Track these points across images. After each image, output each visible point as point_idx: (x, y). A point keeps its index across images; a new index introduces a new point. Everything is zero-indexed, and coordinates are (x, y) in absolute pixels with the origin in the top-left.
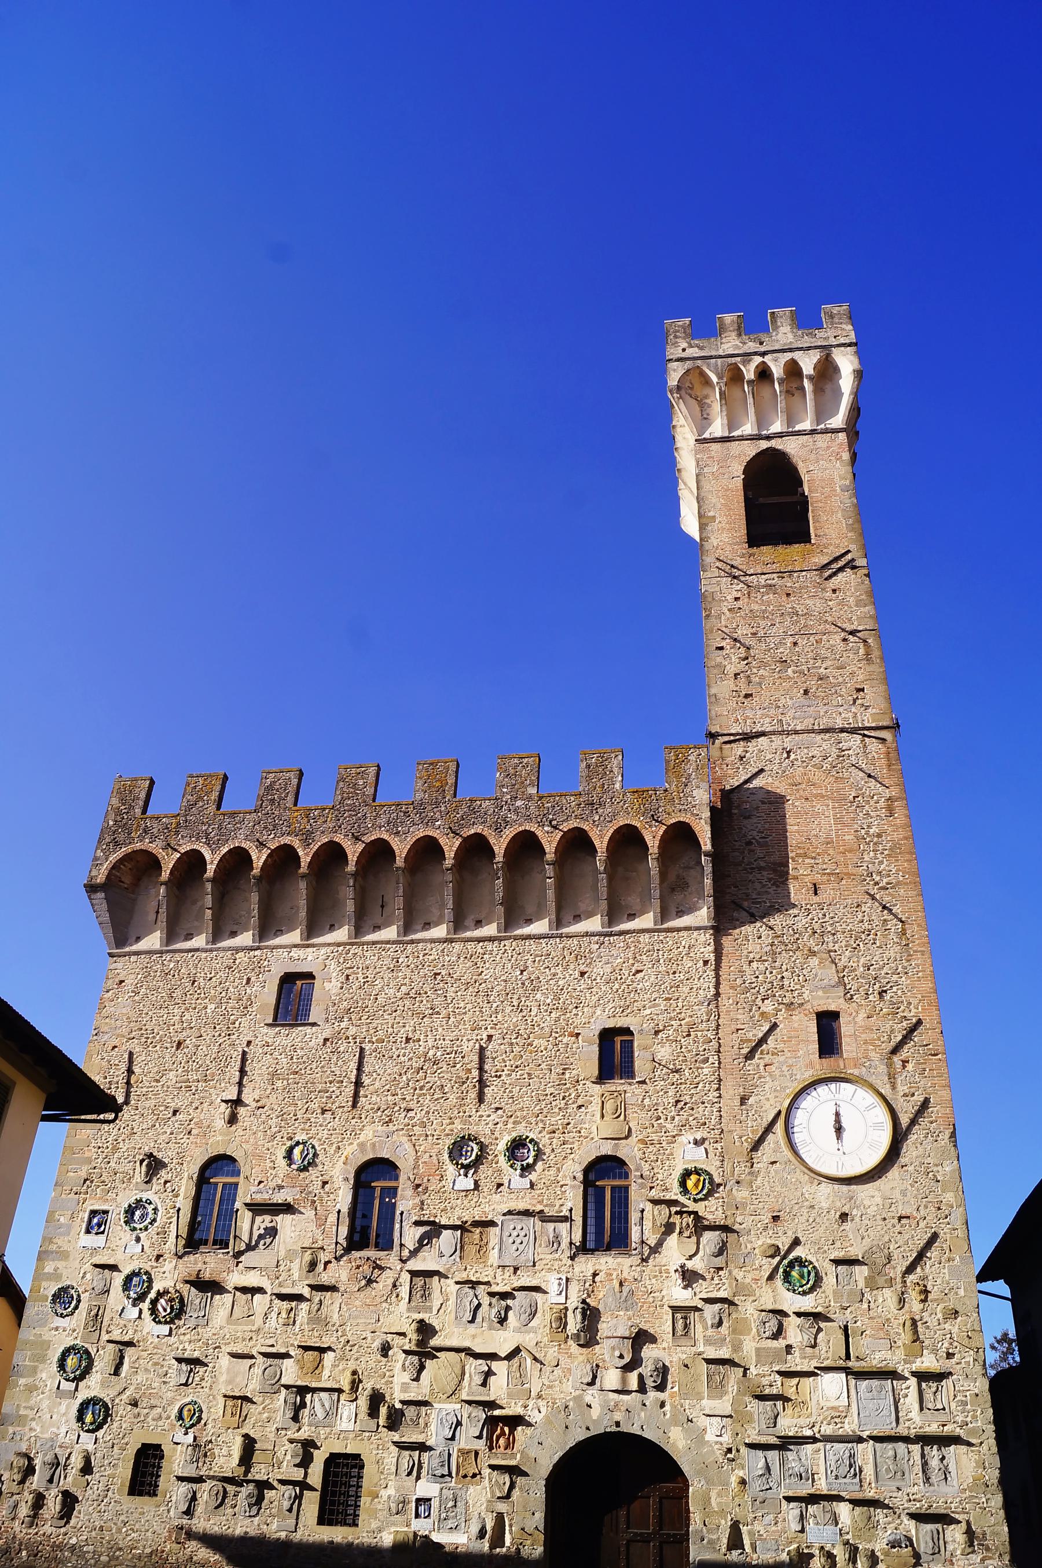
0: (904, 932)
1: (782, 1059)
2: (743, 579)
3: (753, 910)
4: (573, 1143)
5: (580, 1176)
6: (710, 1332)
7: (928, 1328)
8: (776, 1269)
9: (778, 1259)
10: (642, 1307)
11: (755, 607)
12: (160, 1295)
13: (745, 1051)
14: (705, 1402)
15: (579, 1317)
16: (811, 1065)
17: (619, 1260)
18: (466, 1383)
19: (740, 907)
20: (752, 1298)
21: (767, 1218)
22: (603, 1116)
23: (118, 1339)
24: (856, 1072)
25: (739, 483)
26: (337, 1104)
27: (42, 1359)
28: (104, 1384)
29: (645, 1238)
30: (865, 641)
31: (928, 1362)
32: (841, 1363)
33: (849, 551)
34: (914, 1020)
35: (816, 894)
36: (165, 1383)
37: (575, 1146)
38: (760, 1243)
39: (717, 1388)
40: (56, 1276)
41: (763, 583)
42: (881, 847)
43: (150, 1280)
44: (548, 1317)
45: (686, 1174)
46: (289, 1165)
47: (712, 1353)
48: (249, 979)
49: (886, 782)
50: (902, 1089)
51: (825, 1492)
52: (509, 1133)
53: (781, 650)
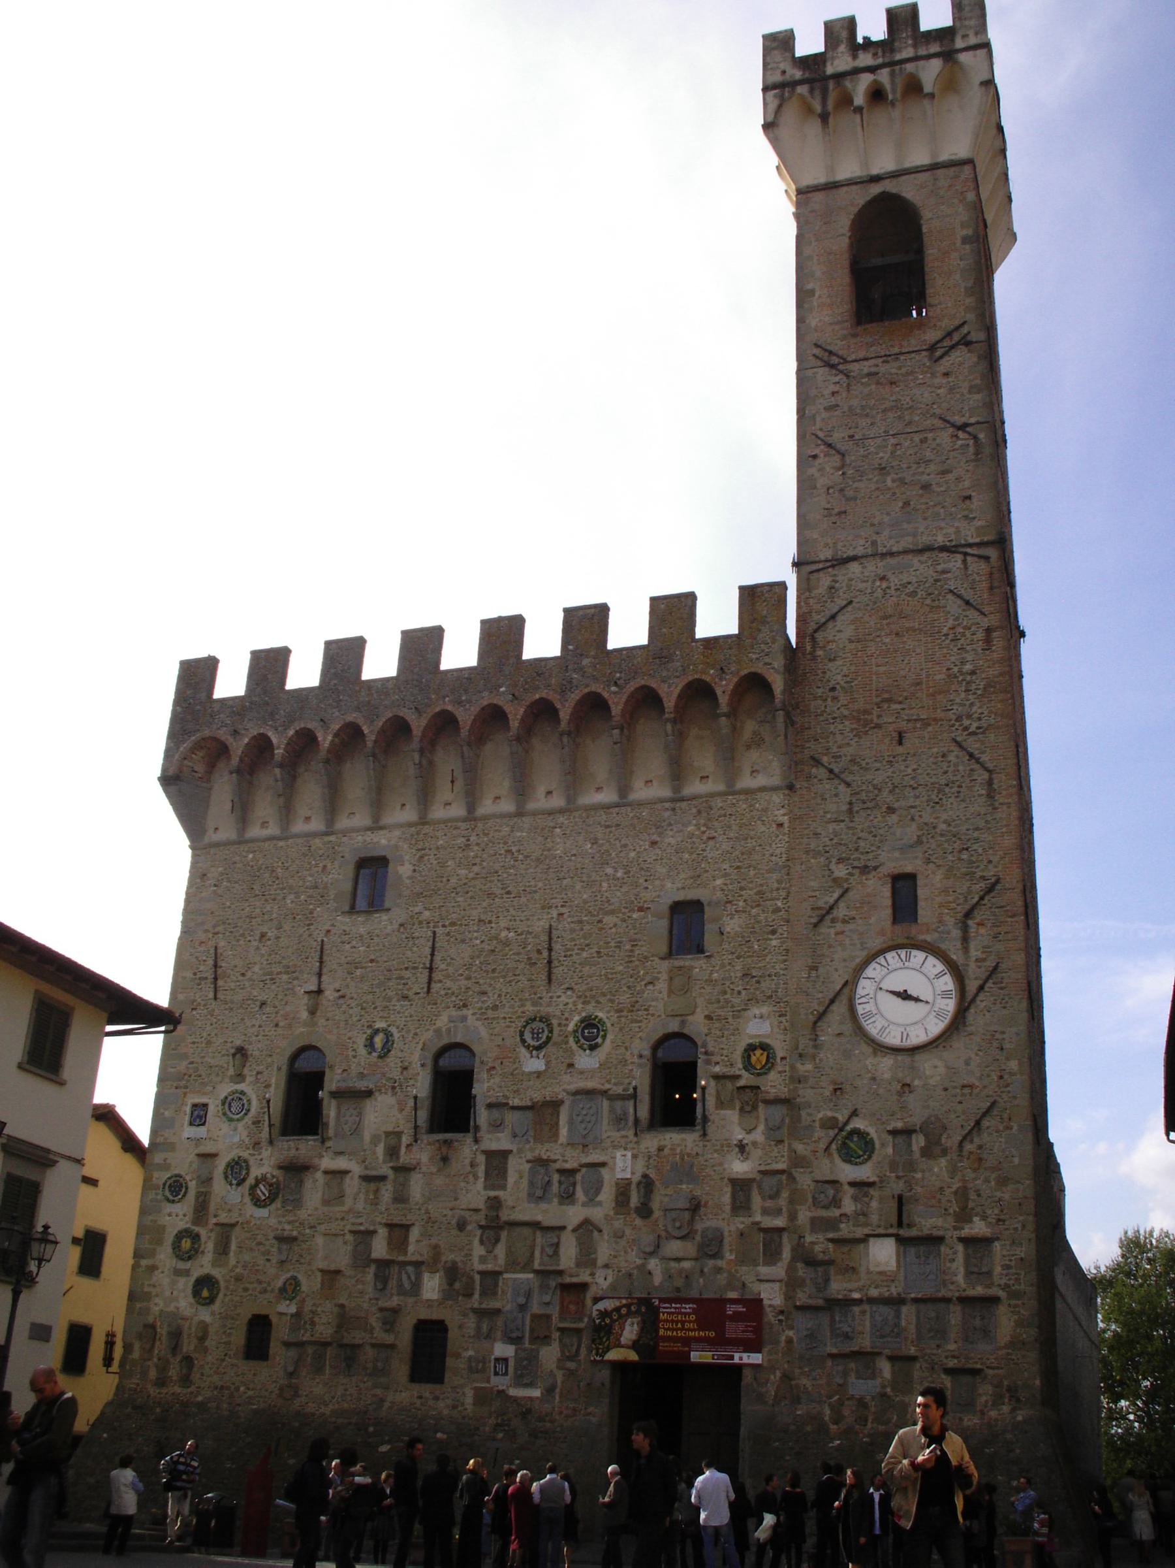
0: (990, 782)
1: (851, 926)
2: (841, 367)
3: (832, 766)
4: (640, 1021)
5: (647, 1053)
6: (769, 1204)
7: (979, 1195)
9: (836, 1131)
11: (855, 402)
12: (258, 1182)
13: (814, 920)
16: (882, 933)
17: (683, 1136)
18: (537, 1254)
19: (817, 762)
22: (671, 992)
23: (225, 1221)
24: (929, 938)
25: (845, 242)
26: (413, 991)
27: (159, 1242)
28: (215, 1264)
30: (975, 438)
31: (978, 1227)
32: (891, 1231)
33: (965, 322)
34: (993, 880)
35: (900, 743)
36: (268, 1260)
37: (643, 1025)
38: (820, 1115)
39: (772, 1255)
40: (165, 1166)
41: (866, 371)
42: (973, 687)
43: (248, 1168)
45: (751, 1048)
46: (370, 1053)
48: (325, 867)
49: (986, 610)
50: (974, 953)
51: (869, 1350)
52: (579, 1013)
53: (881, 455)
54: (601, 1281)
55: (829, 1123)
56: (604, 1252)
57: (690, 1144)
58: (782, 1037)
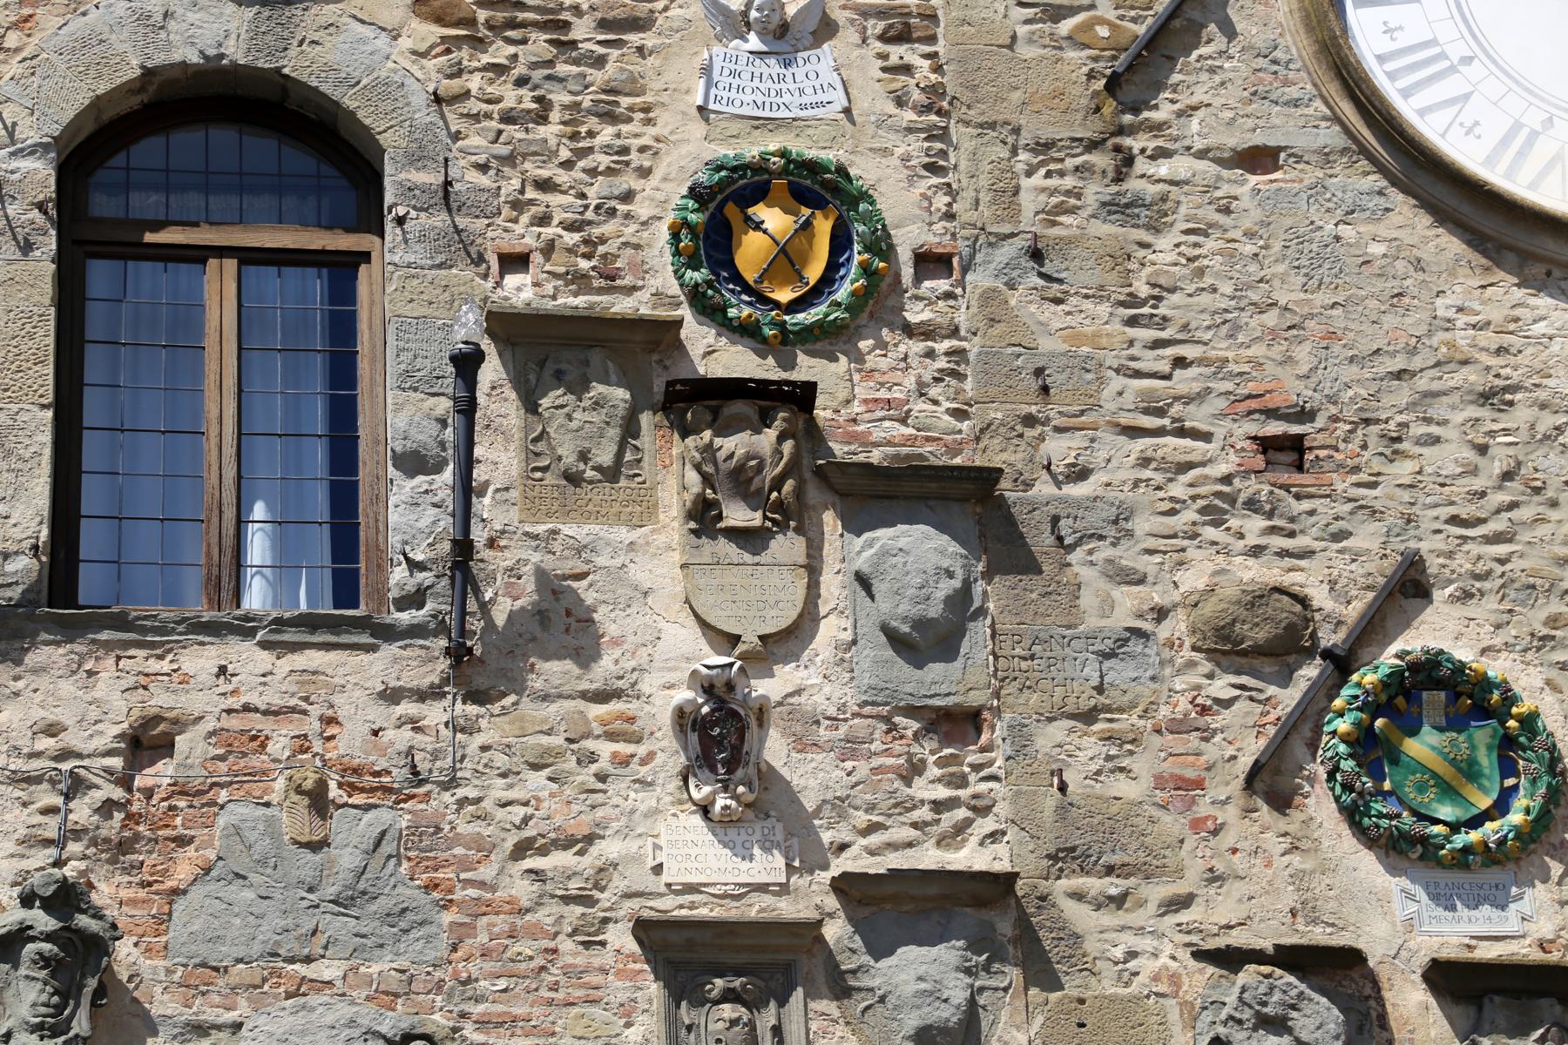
8: (1304, 725)
20: (1158, 892)
21: (1226, 452)
29: (478, 535)
38: (1193, 579)
45: (726, 198)
55: (1260, 640)
57: (359, 715)
58: (916, 146)
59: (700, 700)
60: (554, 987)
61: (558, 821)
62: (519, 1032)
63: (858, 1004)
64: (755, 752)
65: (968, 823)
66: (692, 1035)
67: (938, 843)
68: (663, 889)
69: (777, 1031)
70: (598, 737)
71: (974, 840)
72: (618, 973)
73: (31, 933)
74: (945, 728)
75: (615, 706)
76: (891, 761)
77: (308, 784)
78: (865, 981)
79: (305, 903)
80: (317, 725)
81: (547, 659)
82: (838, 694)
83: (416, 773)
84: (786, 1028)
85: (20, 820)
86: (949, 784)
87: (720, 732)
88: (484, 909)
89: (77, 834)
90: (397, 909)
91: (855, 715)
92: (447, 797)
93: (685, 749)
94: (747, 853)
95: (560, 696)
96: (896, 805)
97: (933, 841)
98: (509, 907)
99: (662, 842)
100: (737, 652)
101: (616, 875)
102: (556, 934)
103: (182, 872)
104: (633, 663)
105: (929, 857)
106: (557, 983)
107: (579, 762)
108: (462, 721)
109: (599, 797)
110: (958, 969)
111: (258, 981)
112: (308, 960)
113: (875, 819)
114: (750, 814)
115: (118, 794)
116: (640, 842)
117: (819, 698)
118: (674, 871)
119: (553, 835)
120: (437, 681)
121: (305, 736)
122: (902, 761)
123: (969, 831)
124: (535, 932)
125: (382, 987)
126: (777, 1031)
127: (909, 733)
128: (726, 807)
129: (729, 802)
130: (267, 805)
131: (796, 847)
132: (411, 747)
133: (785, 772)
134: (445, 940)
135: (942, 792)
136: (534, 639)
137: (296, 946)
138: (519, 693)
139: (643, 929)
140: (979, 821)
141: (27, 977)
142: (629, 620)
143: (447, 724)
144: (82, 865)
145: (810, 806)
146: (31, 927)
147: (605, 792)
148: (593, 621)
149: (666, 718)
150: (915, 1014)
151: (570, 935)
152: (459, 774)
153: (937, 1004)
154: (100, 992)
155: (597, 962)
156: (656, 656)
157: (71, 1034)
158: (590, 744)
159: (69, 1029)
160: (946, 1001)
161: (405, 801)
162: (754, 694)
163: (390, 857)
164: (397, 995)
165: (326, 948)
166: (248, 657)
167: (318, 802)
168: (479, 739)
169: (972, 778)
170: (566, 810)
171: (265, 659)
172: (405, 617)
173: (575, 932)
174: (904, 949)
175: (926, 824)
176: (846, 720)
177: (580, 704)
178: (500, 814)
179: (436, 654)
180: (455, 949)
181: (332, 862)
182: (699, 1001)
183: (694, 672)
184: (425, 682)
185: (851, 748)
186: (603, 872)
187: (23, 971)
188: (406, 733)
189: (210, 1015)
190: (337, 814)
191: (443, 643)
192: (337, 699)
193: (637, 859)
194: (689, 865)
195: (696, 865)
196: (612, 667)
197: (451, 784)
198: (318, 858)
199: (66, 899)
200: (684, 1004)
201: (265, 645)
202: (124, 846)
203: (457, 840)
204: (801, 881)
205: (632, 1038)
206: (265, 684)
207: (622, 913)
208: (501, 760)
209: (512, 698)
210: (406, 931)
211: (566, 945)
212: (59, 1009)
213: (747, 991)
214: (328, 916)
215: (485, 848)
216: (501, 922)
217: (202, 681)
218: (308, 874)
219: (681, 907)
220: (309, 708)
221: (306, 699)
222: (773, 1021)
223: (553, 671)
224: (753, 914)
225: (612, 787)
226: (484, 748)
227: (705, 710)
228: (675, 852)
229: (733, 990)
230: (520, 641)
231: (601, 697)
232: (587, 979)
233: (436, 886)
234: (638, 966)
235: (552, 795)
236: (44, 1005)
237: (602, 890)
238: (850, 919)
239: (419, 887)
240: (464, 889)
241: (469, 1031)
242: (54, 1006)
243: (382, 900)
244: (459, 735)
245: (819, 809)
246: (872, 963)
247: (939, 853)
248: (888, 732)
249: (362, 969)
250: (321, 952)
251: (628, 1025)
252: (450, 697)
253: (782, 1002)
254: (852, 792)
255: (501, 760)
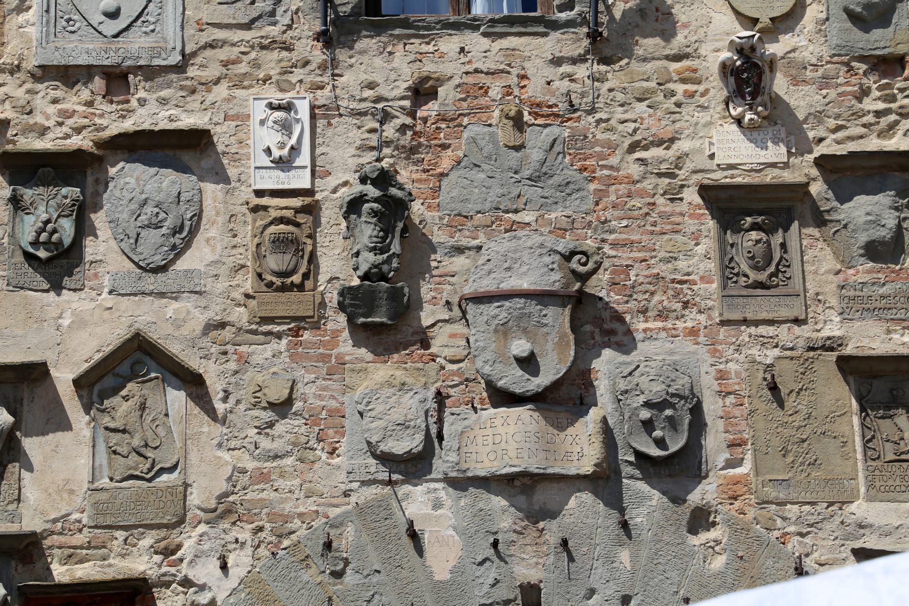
6: (864, 271)
10: (600, 195)
14: (860, 509)
15: (367, 231)
44: (246, 233)
47: (873, 339)
54: (206, 571)
56: (208, 461)
59: (735, 58)
60: (654, 224)
61: (654, 130)
62: (635, 249)
63: (831, 229)
64: (768, 87)
65: (897, 123)
66: (734, 249)
67: (879, 136)
68: (715, 168)
69: (783, 246)
70: (676, 81)
71: (900, 133)
72: (690, 216)
73: (366, 198)
74: (882, 68)
75: (685, 63)
76: (849, 89)
77: (512, 113)
78: (835, 216)
79: (513, 180)
80: (516, 79)
81: (645, 37)
82: (818, 50)
83: (572, 106)
84: (788, 244)
85: (357, 136)
86: (885, 101)
87: (747, 76)
88: (613, 181)
89: (388, 143)
90: (564, 183)
91: (828, 62)
92: (590, 119)
93: (727, 87)
94: (764, 145)
95: (653, 59)
96: (853, 115)
97: (875, 134)
98: (626, 180)
99: (714, 141)
100: (757, 28)
101: (688, 160)
102: (654, 195)
103: (445, 164)
104: (695, 38)
105: (873, 144)
106: (655, 222)
107: (665, 96)
108: (597, 75)
109: (677, 116)
110: (891, 208)
111: (489, 223)
112: (516, 211)
113: (840, 123)
114: (765, 123)
115: (408, 121)
116: (701, 141)
117: (806, 54)
118: (721, 157)
119: (651, 139)
120: (582, 52)
121: (510, 86)
122: (856, 88)
123: (897, 128)
124: (642, 194)
125: (557, 226)
126: (783, 246)
127: (861, 72)
128: (751, 119)
129: (753, 116)
130: (490, 125)
131: (793, 141)
132: (569, 91)
133: (786, 98)
134: (591, 199)
135: (881, 106)
136: (637, 26)
137: (509, 203)
138: (630, 58)
139: (705, 191)
140: (904, 121)
141: (366, 222)
142: (692, 12)
143: (589, 77)
144: (391, 161)
145: (801, 116)
146: (366, 195)
147: (680, 113)
148: (671, 14)
149: (715, 69)
150: (865, 234)
151: (662, 195)
152: (597, 106)
153: (878, 228)
154: (405, 230)
155: (678, 210)
156: (709, 33)
157: (391, 252)
158: (671, 86)
159: (390, 250)
160: (883, 226)
161: (567, 122)
162: (767, 53)
163: (559, 153)
164: (566, 230)
165: (525, 204)
166: (476, 42)
167: (518, 123)
168: (607, 85)
169: (899, 96)
170: (658, 125)
171: (485, 42)
172: (563, 16)
173: (665, 193)
174: (858, 197)
175: (871, 124)
176: (822, 66)
177: (665, 63)
178: (621, 127)
179: (582, 36)
180: (597, 204)
181: (527, 157)
182: (738, 230)
183: (732, 42)
184: (576, 53)
185: (825, 82)
186: (681, 159)
187: (363, 219)
188: (566, 83)
189: (464, 242)
190: (528, 130)
191: (586, 30)
192: (527, 65)
193: (700, 151)
194: (730, 153)
195: (734, 153)
196: (683, 41)
197: (592, 111)
198: (519, 154)
199: (384, 179)
200: (729, 232)
201: (485, 35)
202: (413, 150)
203: (597, 143)
204: (796, 161)
205: (699, 252)
206: (486, 57)
207: (692, 182)
208: (620, 97)
209: (625, 61)
210: (569, 195)
211: (660, 200)
212: (384, 239)
213: (765, 224)
214: (526, 187)
215: (613, 147)
216: (623, 189)
217: (453, 55)
218: (514, 164)
219: (726, 177)
220: (511, 70)
221: (509, 65)
222: (781, 240)
223: (649, 44)
224: (768, 180)
225: (684, 110)
226: (610, 90)
227: (738, 63)
228: (721, 146)
229: (757, 223)
230: (630, 27)
231: (677, 58)
232: (673, 219)
233: (586, 169)
234: (702, 211)
235: (650, 116)
236: (375, 237)
237: (680, 169)
238: (826, 181)
239: (576, 170)
240: (601, 170)
241: (607, 249)
242: (381, 238)
243: (555, 178)
244: (596, 83)
245: (806, 118)
246: (839, 206)
247: (879, 141)
248: (848, 71)
249: (546, 216)
250: (523, 207)
251: (697, 244)
252: (590, 61)
253: (786, 229)
254: (826, 108)
255: (620, 97)
